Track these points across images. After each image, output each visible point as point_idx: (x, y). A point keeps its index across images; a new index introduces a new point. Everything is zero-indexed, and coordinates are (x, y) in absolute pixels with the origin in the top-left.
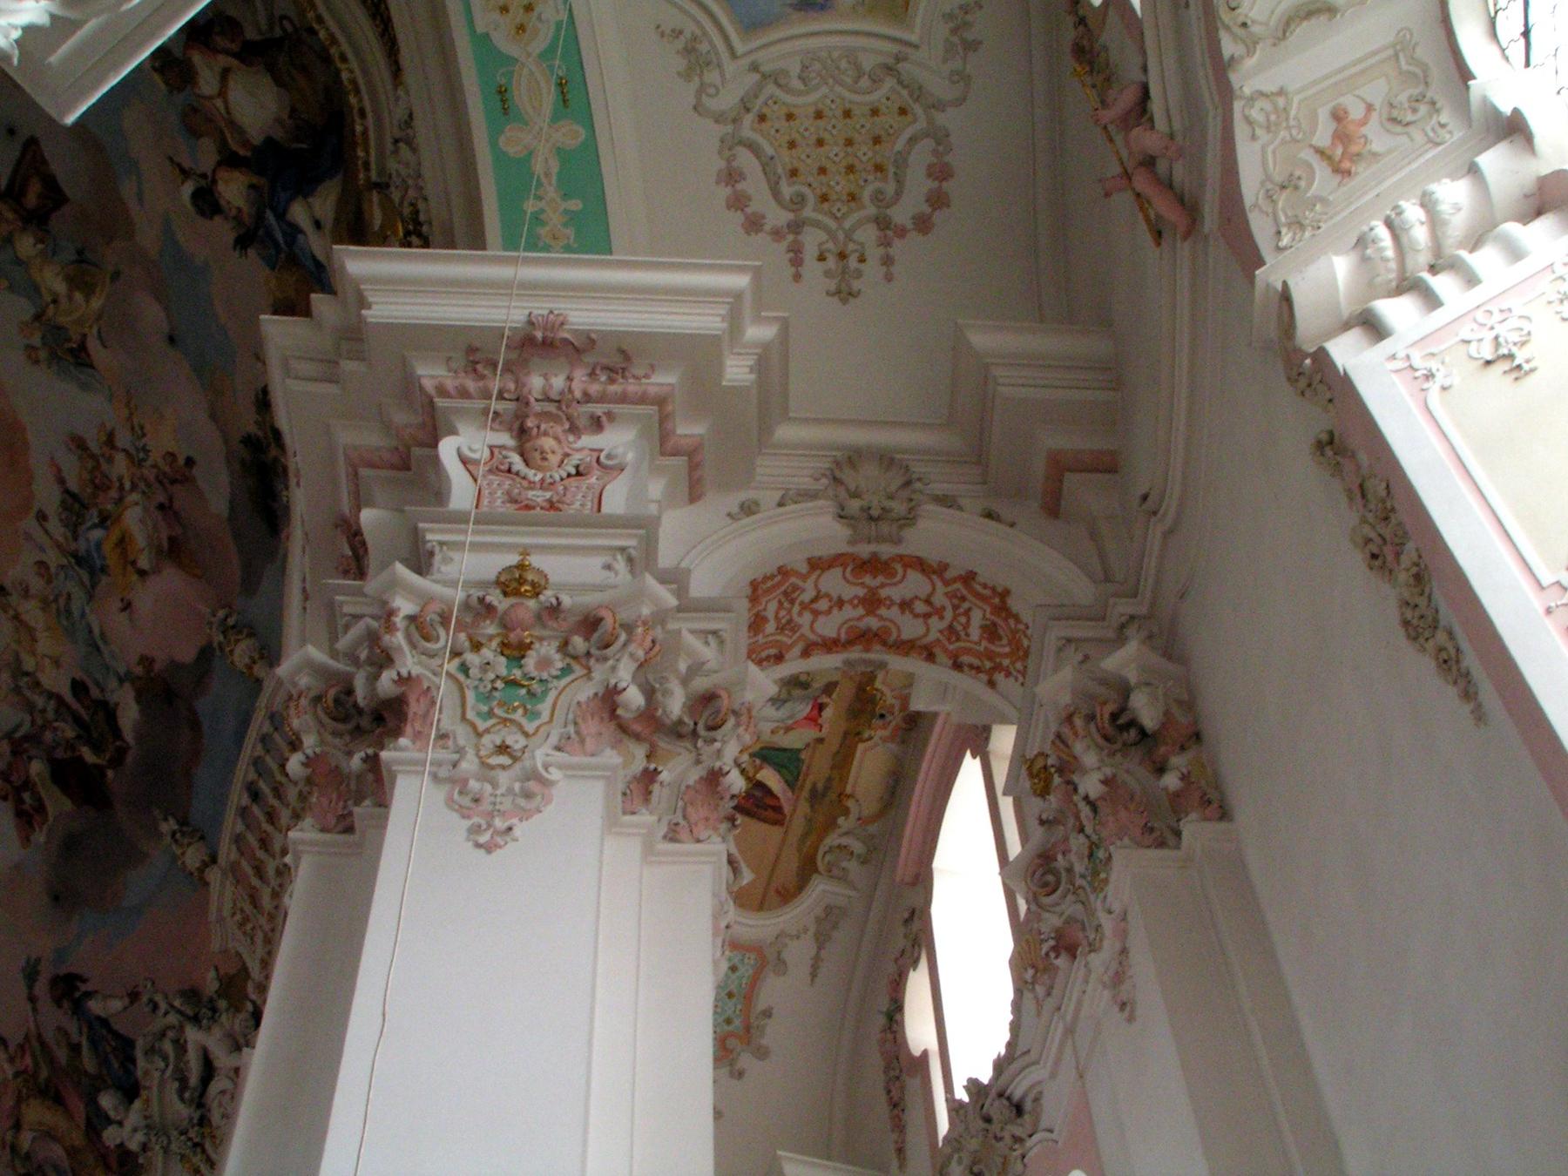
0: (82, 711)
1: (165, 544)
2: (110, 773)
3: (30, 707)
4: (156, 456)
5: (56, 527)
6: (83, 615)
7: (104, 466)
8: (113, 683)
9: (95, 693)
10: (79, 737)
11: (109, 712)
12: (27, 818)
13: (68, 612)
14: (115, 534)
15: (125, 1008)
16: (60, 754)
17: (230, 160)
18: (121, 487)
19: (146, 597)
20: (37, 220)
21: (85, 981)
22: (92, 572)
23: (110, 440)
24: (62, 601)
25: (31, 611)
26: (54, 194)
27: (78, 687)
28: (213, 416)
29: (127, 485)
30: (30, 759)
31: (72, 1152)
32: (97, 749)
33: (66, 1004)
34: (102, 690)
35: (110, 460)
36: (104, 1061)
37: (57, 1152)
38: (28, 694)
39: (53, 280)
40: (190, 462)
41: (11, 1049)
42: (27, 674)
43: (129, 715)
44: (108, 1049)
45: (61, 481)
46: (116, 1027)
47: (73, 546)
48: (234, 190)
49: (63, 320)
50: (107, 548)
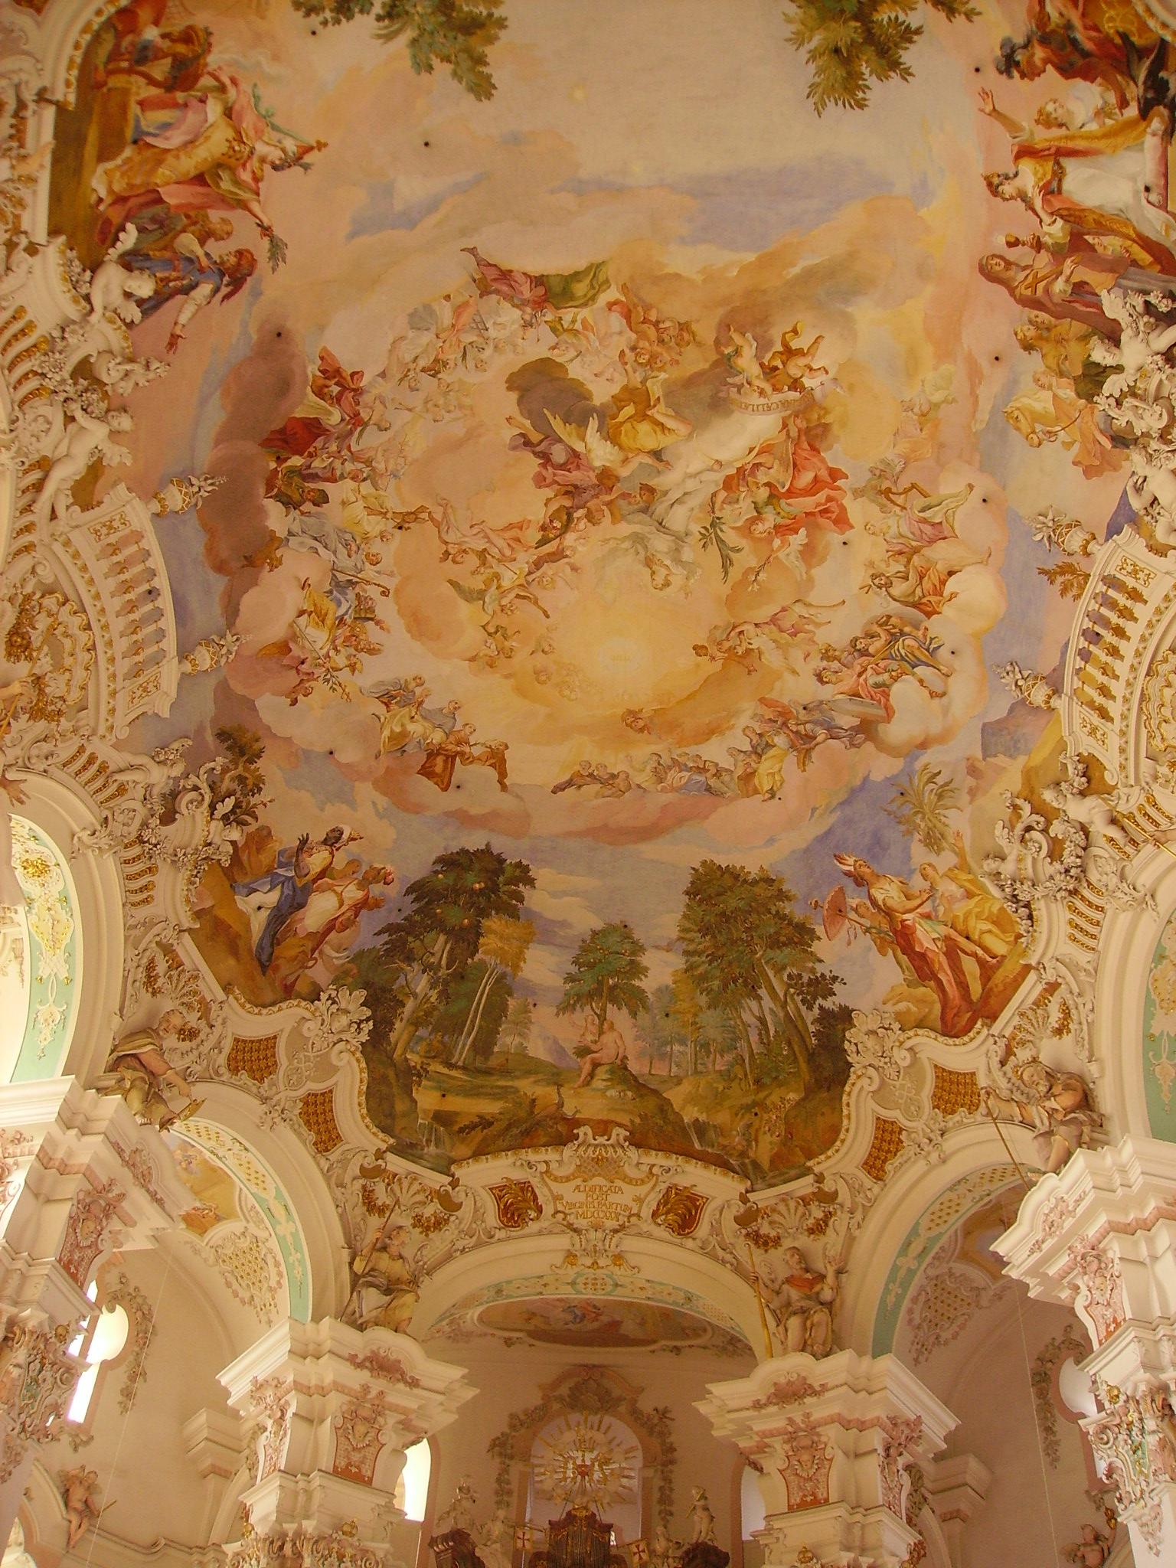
0: (312, 486)
1: (291, 645)
2: (273, 465)
3: (355, 458)
4: (320, 687)
5: (373, 592)
6: (335, 553)
7: (352, 651)
8: (296, 528)
9: (307, 507)
10: (309, 467)
11: (290, 504)
12: (331, 372)
13: (346, 545)
14: (329, 622)
15: (176, 324)
16: (319, 443)
17: (322, 874)
18: (335, 649)
19: (294, 599)
20: (432, 754)
21: (227, 297)
22: (337, 584)
23: (353, 668)
24: (354, 548)
25: (374, 525)
26: (426, 772)
27: (322, 499)
28: (288, 740)
29: (332, 653)
30: (342, 420)
32: (292, 471)
33: (233, 260)
34: (303, 513)
35: (348, 657)
38: (361, 466)
39: (416, 728)
40: (294, 702)
41: (267, 167)
42: (364, 480)
43: (276, 518)
44: (174, 274)
45: (377, 623)
46: (180, 297)
47: (358, 589)
48: (316, 861)
49: (407, 709)
50: (333, 606)
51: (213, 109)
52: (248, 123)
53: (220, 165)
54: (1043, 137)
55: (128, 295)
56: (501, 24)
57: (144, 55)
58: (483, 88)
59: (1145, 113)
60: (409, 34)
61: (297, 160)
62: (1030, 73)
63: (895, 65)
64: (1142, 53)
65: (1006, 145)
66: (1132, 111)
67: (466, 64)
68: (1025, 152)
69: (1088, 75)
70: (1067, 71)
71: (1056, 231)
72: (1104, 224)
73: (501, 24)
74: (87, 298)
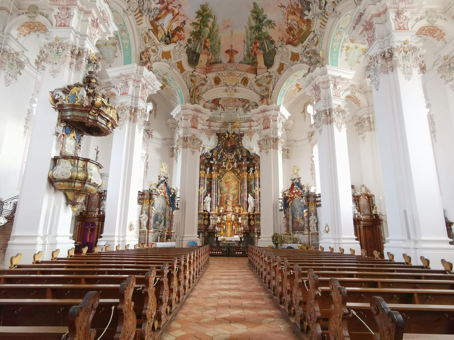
31: (297, 22)
36: (303, 6)
37: (295, 22)
51: (289, 21)
52: (286, 16)
53: (292, 14)
54: (177, 17)
55: (309, 10)
56: (251, 11)
57: (293, 36)
58: (255, 4)
59: (168, 32)
60: (263, 14)
61: (282, 6)
62: (181, 24)
63: (198, 13)
64: (172, 37)
65: (181, 13)
66: (169, 31)
67: (257, 8)
68: (178, 14)
69: (176, 29)
70: (178, 27)
71: (170, 7)
72: (165, 14)
73: (251, 11)
74: (313, 18)
